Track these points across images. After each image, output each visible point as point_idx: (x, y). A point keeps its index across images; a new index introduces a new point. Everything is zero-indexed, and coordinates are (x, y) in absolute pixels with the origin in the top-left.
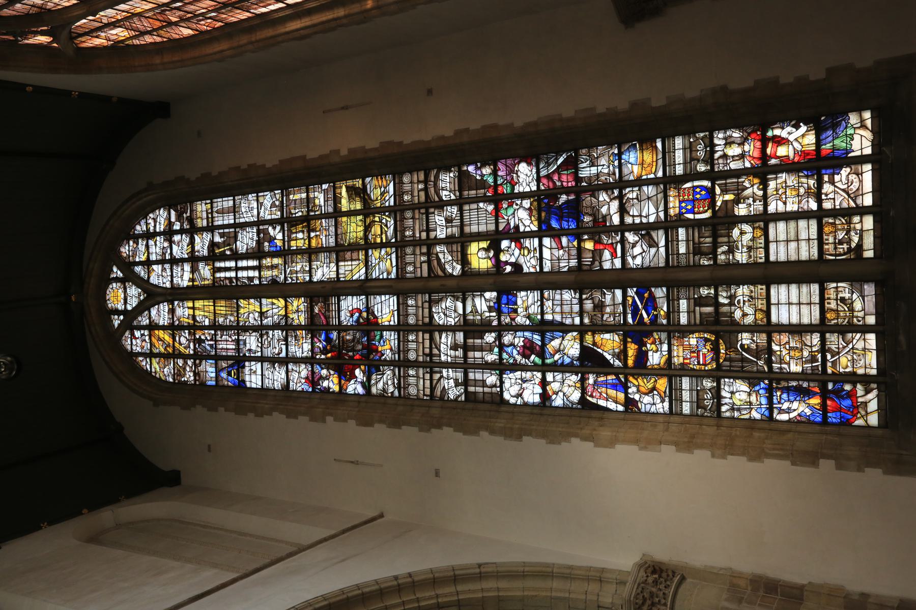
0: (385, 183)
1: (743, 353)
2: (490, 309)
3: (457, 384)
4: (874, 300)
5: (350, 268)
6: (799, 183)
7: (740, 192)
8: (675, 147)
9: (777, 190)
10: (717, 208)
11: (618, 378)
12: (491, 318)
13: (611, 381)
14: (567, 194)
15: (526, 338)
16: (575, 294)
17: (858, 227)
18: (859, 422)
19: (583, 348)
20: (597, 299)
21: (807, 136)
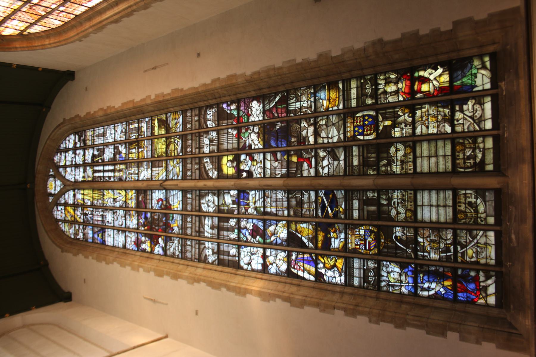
0: (177, 117)
1: (397, 243)
2: (234, 202)
3: (213, 253)
4: (493, 204)
5: (157, 172)
6: (437, 112)
7: (395, 119)
8: (351, 86)
9: (422, 117)
10: (379, 132)
11: (311, 256)
12: (234, 209)
13: (306, 259)
15: (254, 224)
16: (285, 194)
17: (481, 145)
18: (481, 301)
19: (289, 233)
20: (299, 198)
21: (443, 76)
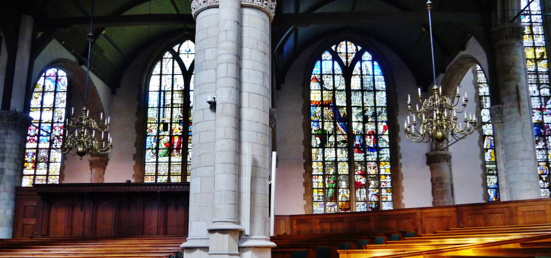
3: (485, 93)
9: (546, 191)
11: (493, 147)
14: (544, 133)
